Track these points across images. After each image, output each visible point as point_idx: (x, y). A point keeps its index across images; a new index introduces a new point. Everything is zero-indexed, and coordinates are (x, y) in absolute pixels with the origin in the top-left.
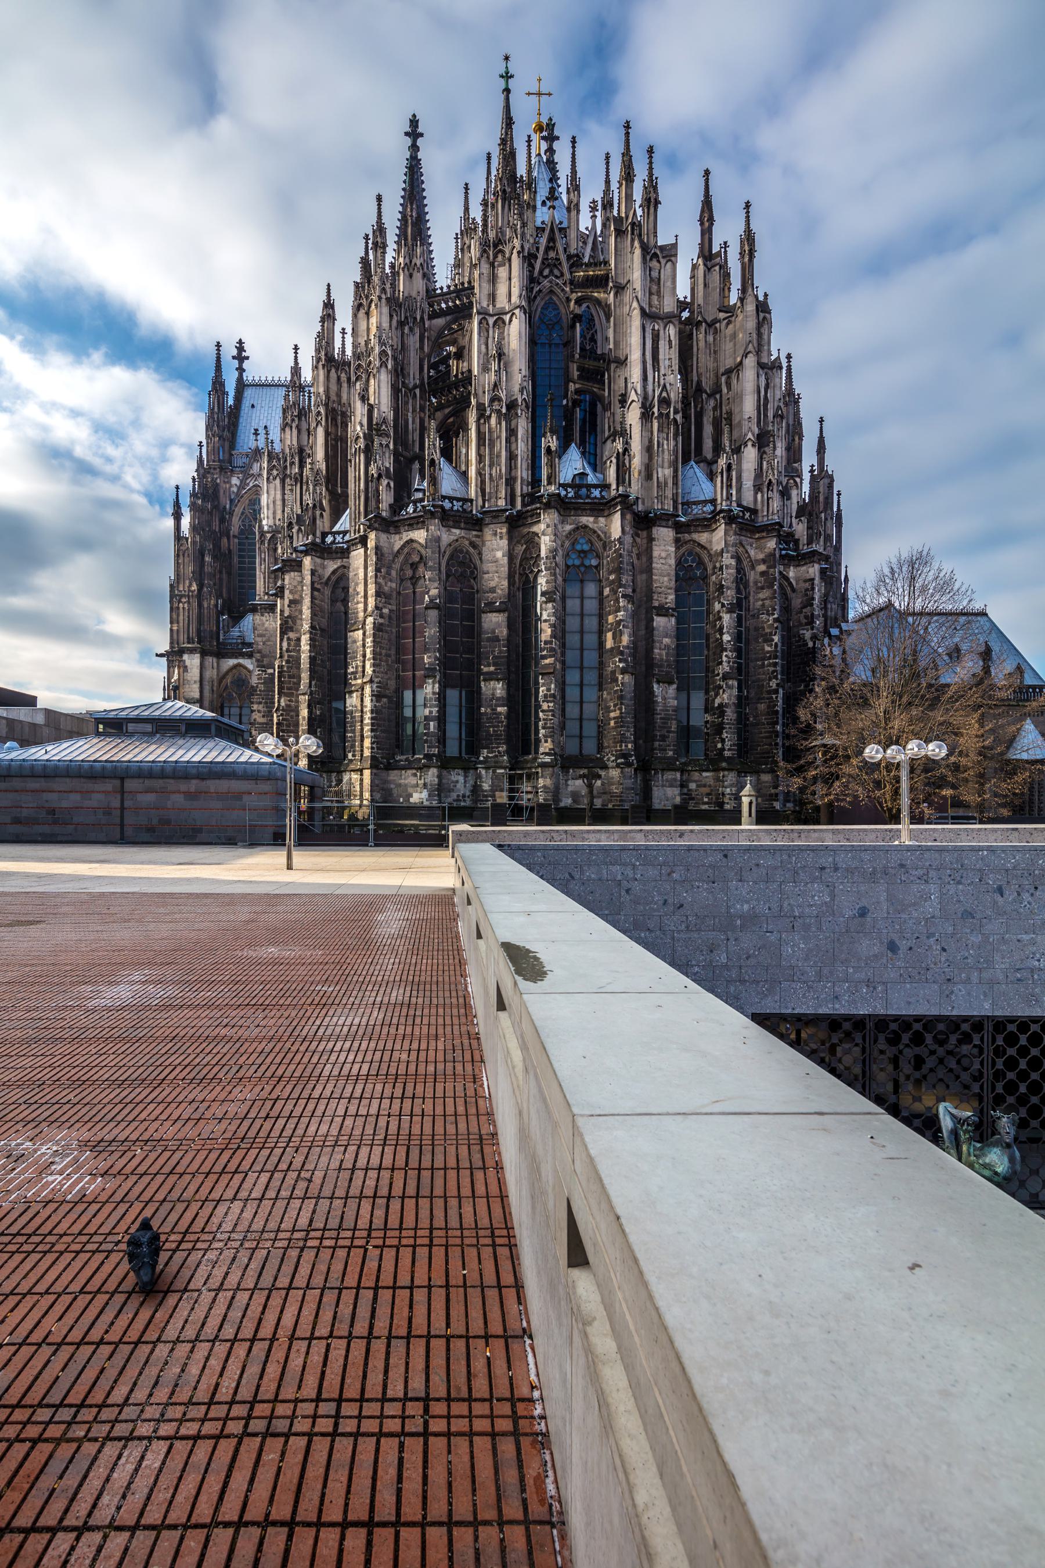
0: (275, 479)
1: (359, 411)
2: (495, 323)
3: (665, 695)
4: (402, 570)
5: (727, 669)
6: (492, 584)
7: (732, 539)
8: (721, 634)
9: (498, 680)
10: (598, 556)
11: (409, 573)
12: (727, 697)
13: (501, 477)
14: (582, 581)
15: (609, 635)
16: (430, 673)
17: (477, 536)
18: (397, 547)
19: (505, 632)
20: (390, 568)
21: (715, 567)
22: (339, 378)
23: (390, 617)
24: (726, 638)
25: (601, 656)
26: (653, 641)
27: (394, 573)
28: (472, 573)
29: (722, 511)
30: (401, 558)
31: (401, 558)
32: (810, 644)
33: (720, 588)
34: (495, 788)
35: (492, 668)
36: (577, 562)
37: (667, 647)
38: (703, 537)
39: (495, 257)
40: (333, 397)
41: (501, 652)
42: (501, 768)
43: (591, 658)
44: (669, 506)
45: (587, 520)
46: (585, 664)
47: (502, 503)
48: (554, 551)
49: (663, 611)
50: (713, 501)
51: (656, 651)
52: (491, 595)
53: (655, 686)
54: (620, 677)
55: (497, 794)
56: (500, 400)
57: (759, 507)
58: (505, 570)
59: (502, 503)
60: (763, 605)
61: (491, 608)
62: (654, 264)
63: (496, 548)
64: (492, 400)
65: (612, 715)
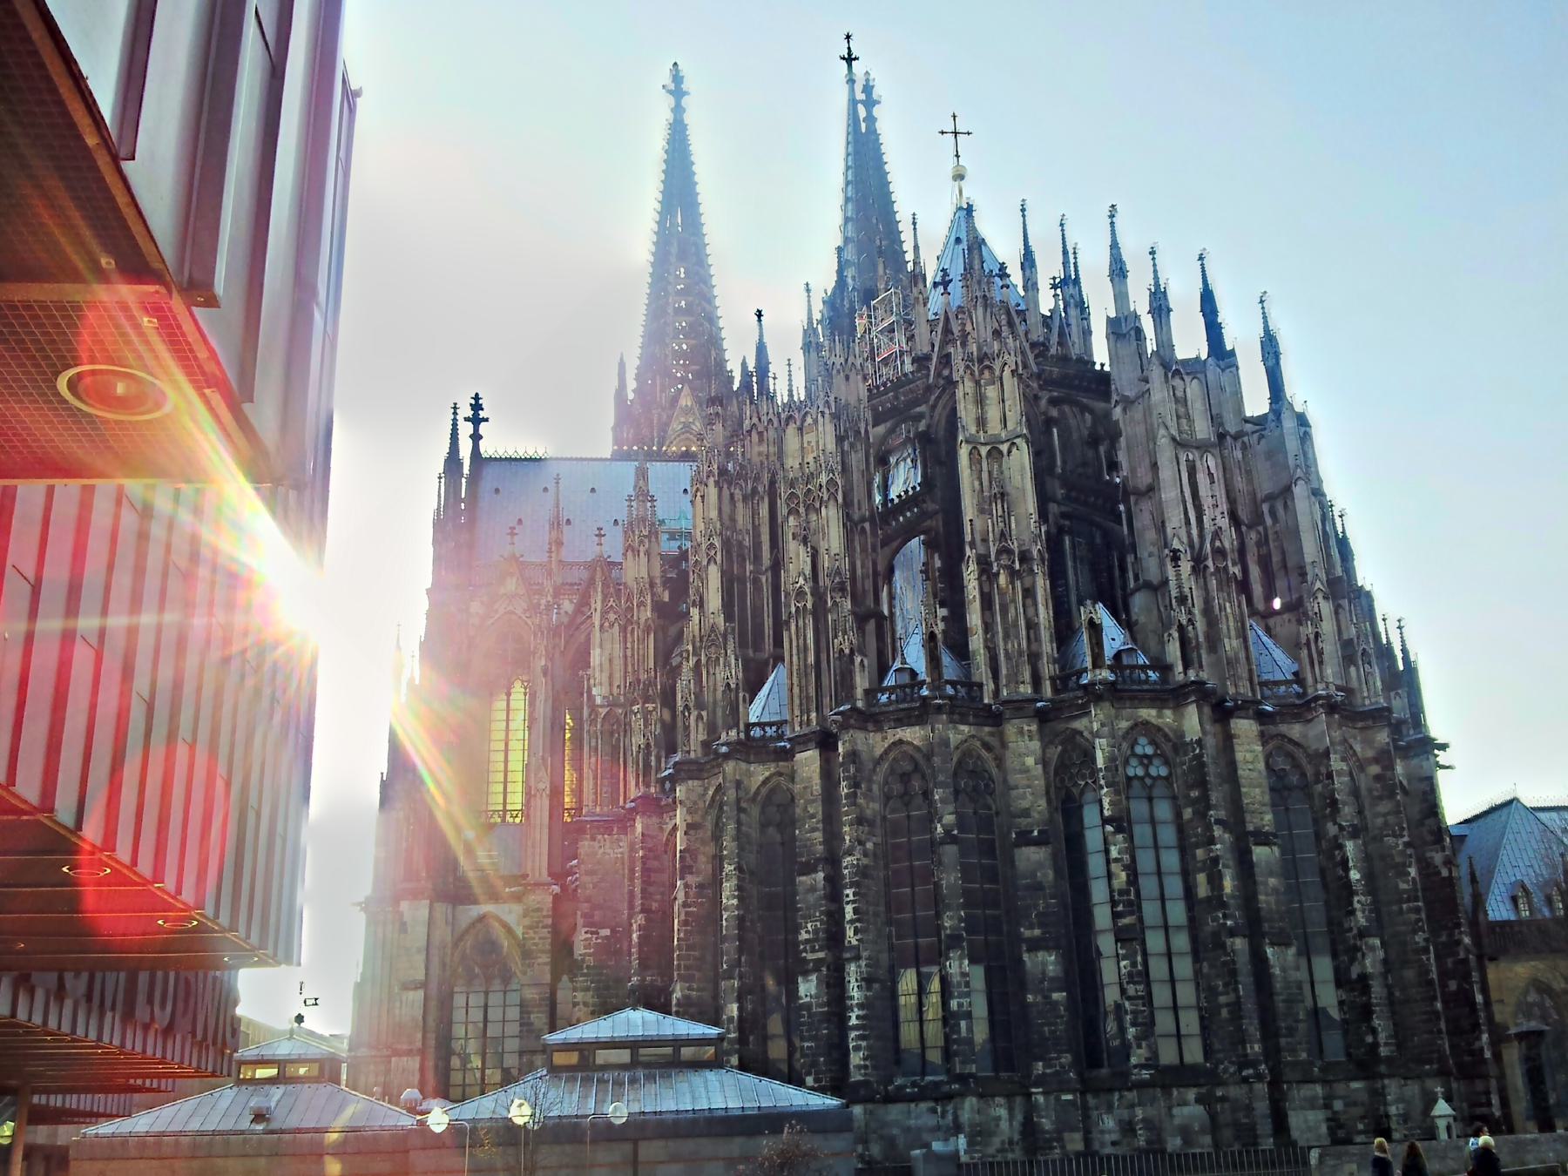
1: (798, 559)
4: (886, 783)
8: (1347, 870)
9: (1047, 949)
11: (897, 788)
12: (1371, 963)
15: (1201, 878)
16: (955, 941)
18: (878, 751)
20: (870, 781)
21: (1317, 774)
22: (732, 496)
23: (875, 855)
24: (1355, 875)
26: (1255, 883)
27: (875, 787)
28: (987, 786)
35: (1037, 932)
37: (1275, 891)
38: (1295, 730)
40: (727, 523)
41: (1047, 906)
43: (1177, 912)
44: (1245, 689)
46: (1171, 923)
49: (1263, 839)
51: (1262, 897)
52: (1023, 822)
53: (1269, 951)
54: (1229, 941)
57: (1354, 684)
61: (1025, 839)
62: (1177, 382)
65: (1223, 999)
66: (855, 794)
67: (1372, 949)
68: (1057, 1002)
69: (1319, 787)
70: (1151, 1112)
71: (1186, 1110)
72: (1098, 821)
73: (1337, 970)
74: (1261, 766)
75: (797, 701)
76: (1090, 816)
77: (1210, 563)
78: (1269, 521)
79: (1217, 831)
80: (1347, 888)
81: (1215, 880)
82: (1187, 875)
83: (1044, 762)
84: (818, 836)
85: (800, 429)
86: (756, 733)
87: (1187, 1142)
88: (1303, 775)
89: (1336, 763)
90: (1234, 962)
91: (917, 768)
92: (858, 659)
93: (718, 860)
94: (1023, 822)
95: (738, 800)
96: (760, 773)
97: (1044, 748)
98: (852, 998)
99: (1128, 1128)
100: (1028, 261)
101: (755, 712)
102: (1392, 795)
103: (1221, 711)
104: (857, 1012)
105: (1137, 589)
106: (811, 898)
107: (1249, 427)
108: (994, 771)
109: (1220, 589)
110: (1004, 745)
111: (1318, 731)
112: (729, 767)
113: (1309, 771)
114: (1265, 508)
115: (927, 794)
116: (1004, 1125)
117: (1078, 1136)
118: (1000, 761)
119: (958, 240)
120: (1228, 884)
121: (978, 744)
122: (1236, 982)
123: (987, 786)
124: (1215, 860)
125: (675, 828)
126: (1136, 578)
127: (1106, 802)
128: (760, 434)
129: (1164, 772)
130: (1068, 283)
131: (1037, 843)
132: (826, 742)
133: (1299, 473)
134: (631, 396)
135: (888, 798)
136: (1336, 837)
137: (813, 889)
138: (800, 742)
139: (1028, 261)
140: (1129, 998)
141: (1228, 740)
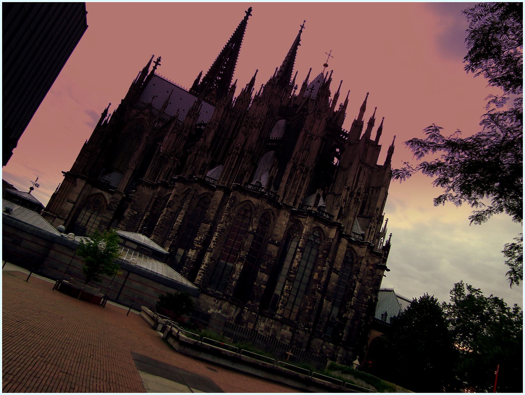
0: (174, 133)
1: (241, 138)
2: (309, 137)
3: (327, 304)
5: (352, 304)
6: (277, 233)
7: (368, 254)
9: (266, 274)
10: (320, 241)
11: (242, 213)
13: (294, 193)
14: (312, 248)
15: (316, 274)
16: (241, 260)
17: (276, 211)
19: (276, 255)
21: (357, 262)
22: (227, 114)
24: (356, 291)
25: (310, 280)
26: (329, 282)
27: (236, 209)
28: (268, 224)
29: (368, 243)
30: (242, 205)
31: (242, 205)
32: (374, 301)
33: (358, 272)
34: (249, 320)
35: (265, 267)
36: (312, 239)
38: (356, 248)
39: (317, 115)
42: (255, 312)
43: (306, 279)
45: (322, 226)
47: (291, 204)
48: (307, 232)
49: (336, 272)
50: (363, 235)
52: (275, 238)
53: (325, 300)
54: (317, 293)
55: (249, 323)
56: (303, 165)
58: (284, 230)
59: (291, 204)
60: (368, 282)
61: (273, 242)
63: (283, 221)
64: (301, 164)
65: (308, 307)
66: (230, 209)
67: (352, 312)
68: (262, 288)
69: (356, 265)
70: (276, 328)
71: (285, 331)
72: (295, 246)
73: (339, 313)
74: (344, 253)
75: (223, 176)
76: (293, 245)
77: (355, 195)
78: (370, 193)
79: (327, 264)
80: (352, 294)
81: (320, 276)
82: (313, 271)
83: (287, 226)
84: (213, 215)
85: (258, 104)
86: (207, 179)
87: (282, 339)
88: (353, 260)
89: (364, 261)
90: (316, 299)
91: (251, 210)
92: (247, 173)
93: (180, 209)
94: (275, 238)
95: (194, 194)
96: (204, 191)
97: (289, 221)
98: (204, 261)
99: (267, 329)
100: (337, 96)
101: (209, 174)
102: (373, 276)
103: (340, 235)
104: (204, 265)
105: (330, 193)
106: (203, 230)
107: (376, 167)
108: (272, 221)
109: (354, 203)
110: (278, 215)
111: (362, 251)
112: (195, 185)
113: (355, 260)
114: (371, 189)
115: (250, 218)
116: (233, 313)
117: (252, 325)
118: (275, 219)
119: (319, 81)
120: (323, 279)
121: (271, 211)
122: (314, 305)
123: (268, 224)
124: (323, 271)
125: (171, 194)
126: (331, 190)
127: (301, 243)
128: (243, 102)
129: (319, 242)
130: (344, 107)
131: (276, 245)
132: (227, 192)
133: (385, 185)
134: (199, 83)
135: (239, 214)
136: (355, 280)
137: (205, 228)
138: (219, 188)
139: (337, 96)
140: (284, 296)
141: (339, 241)
